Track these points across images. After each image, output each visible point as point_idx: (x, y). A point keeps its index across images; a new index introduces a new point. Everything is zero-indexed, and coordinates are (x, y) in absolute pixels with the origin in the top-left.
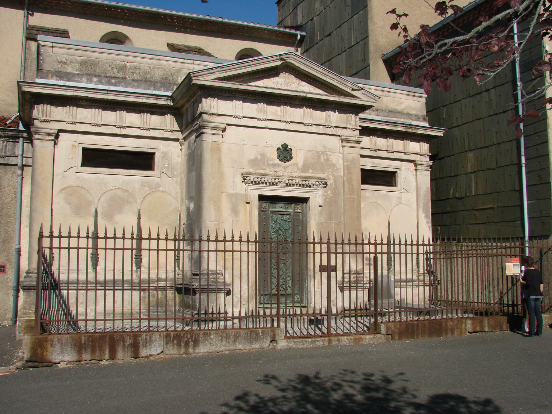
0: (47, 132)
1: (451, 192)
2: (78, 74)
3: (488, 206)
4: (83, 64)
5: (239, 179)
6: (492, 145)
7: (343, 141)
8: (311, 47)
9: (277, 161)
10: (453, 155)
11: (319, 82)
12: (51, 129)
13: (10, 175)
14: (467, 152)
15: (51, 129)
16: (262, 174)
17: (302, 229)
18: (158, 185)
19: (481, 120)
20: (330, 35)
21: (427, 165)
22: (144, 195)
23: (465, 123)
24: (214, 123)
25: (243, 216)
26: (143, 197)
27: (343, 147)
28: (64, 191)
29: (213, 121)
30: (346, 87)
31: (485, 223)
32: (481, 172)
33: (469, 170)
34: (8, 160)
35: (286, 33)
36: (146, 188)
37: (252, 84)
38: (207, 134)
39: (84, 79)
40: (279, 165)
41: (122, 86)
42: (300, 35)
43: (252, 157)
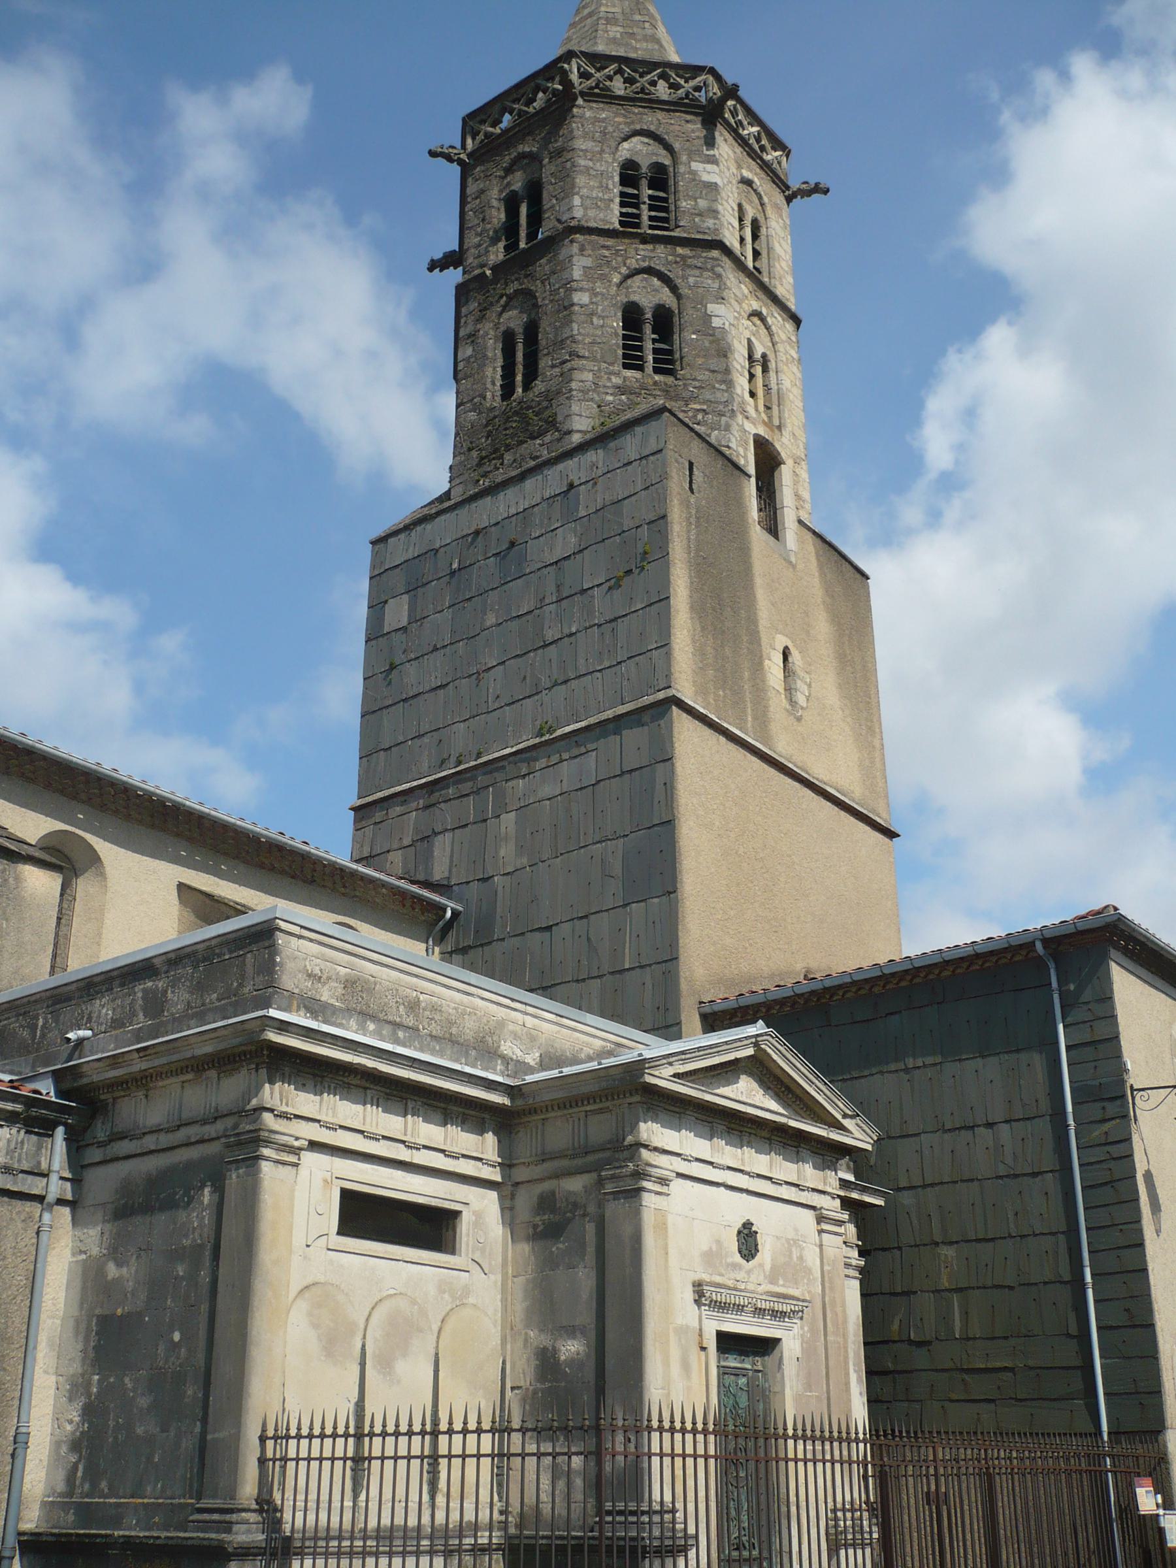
0: (289, 1143)
1: (895, 1326)
2: (341, 1009)
3: (998, 1365)
4: (350, 984)
5: (689, 1295)
6: (1005, 1238)
7: (820, 1219)
8: (482, 945)
9: (738, 1258)
10: (899, 1248)
11: (788, 1089)
12: (297, 1139)
13: (20, 1225)
14: (937, 1244)
15: (297, 1139)
16: (719, 1284)
17: (765, 1410)
18: (467, 1291)
19: (976, 1183)
20: (549, 928)
21: (857, 1267)
22: (443, 1314)
23: (932, 1185)
24: (661, 1168)
25: (698, 1380)
26: (440, 1318)
27: (821, 1232)
28: (307, 1295)
29: (654, 1163)
30: (834, 1109)
31: (992, 1401)
32: (977, 1292)
33: (945, 1283)
34: (24, 1181)
35: (420, 899)
36: (446, 1296)
37: (720, 1091)
38: (650, 1191)
39: (353, 1023)
40: (740, 1267)
41: (416, 1049)
42: (452, 909)
43: (705, 1248)
